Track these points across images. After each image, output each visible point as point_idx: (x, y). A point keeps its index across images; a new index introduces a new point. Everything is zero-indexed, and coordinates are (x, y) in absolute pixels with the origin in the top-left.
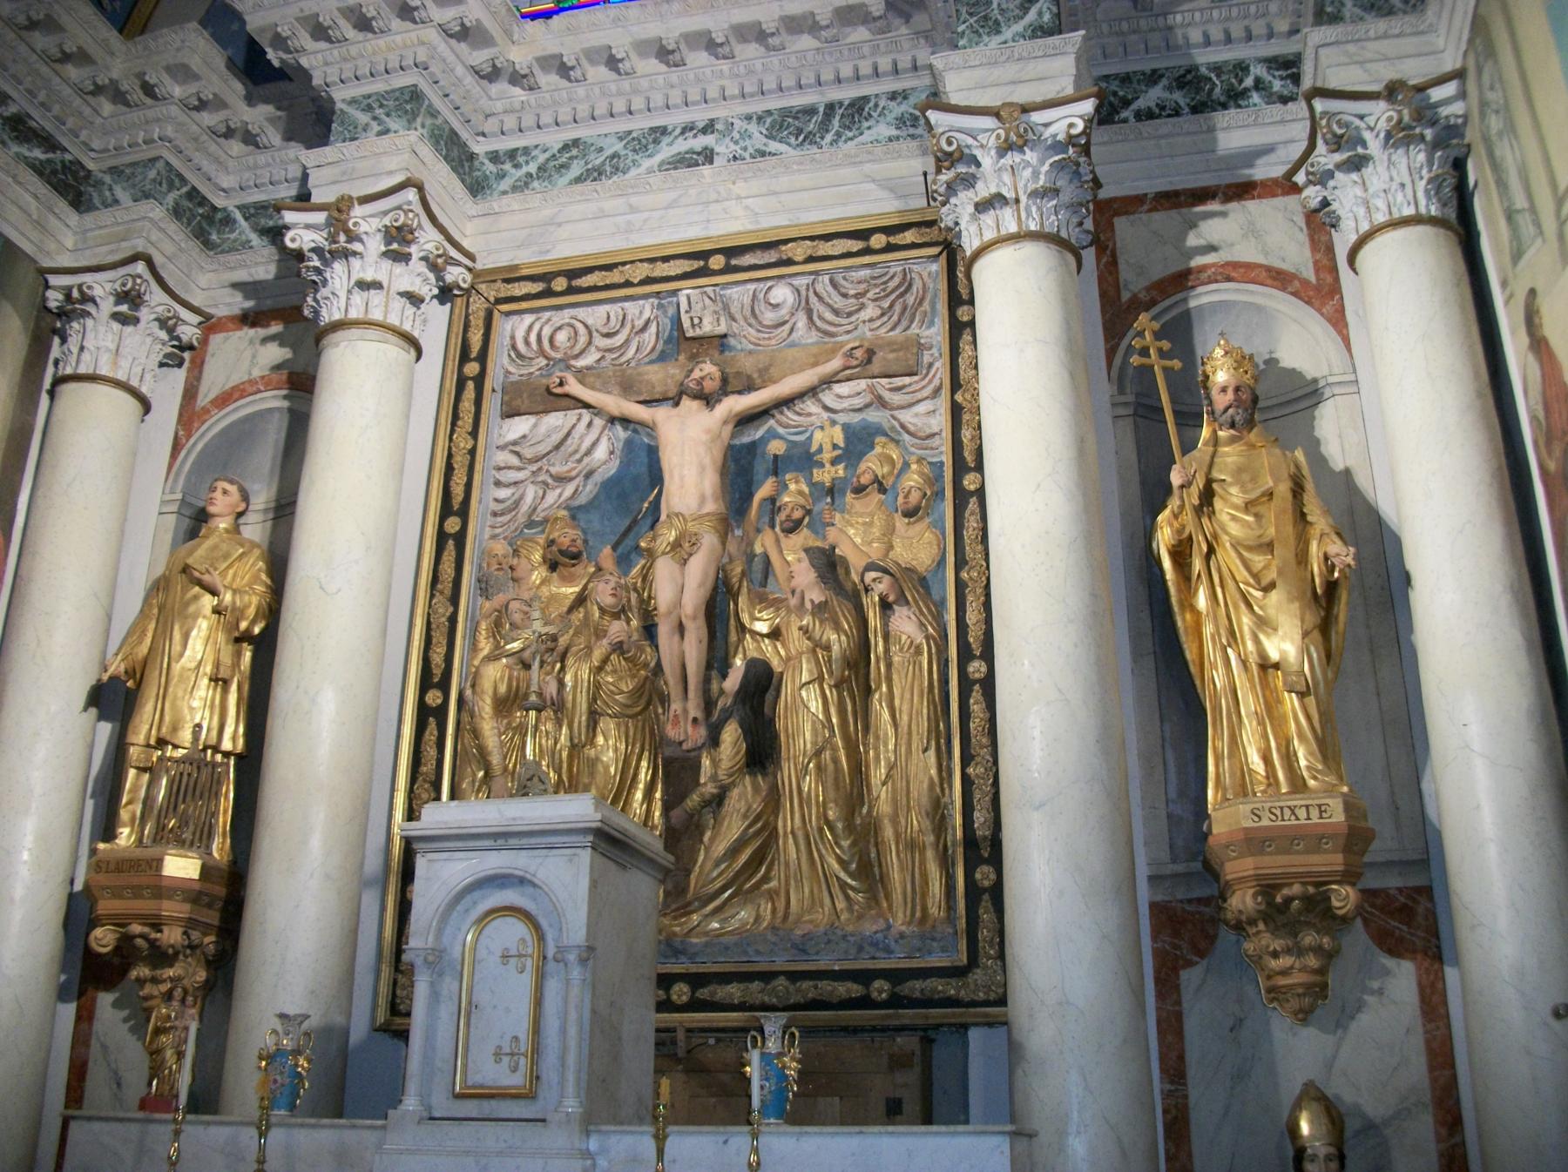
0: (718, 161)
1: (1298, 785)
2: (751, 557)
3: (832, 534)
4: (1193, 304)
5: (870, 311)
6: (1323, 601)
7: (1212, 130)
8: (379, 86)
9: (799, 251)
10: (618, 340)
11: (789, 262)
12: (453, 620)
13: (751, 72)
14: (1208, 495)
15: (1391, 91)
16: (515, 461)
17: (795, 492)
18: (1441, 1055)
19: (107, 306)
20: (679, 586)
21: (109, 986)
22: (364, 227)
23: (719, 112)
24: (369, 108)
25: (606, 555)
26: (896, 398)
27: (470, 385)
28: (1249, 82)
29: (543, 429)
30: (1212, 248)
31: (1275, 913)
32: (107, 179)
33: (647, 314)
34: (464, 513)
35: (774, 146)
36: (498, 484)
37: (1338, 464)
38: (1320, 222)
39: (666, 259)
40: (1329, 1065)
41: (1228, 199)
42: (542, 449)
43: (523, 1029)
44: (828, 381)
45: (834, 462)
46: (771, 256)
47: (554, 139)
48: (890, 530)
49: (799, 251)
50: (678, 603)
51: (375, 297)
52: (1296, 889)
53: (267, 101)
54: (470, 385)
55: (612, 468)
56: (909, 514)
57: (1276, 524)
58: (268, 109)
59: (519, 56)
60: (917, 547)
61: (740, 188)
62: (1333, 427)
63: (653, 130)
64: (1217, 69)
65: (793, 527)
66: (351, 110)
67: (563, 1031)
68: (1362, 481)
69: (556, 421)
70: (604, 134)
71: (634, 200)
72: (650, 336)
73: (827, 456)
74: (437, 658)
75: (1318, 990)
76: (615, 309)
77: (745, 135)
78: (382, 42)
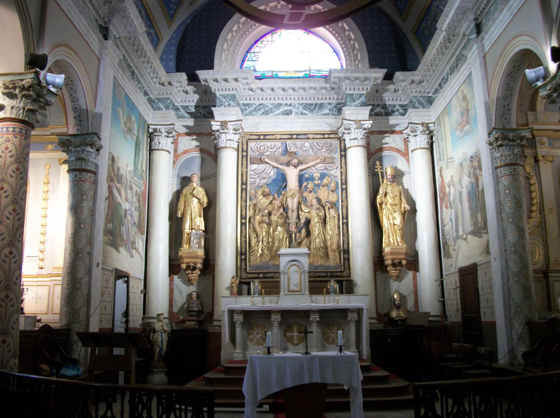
0: (293, 114)
1: (398, 245)
2: (303, 197)
3: (318, 194)
4: (383, 154)
5: (324, 150)
6: (403, 214)
7: (388, 119)
8: (227, 93)
9: (311, 136)
10: (274, 150)
11: (309, 138)
12: (246, 206)
13: (301, 95)
14: (386, 194)
15: (423, 124)
16: (254, 173)
17: (310, 185)
18: (415, 286)
19: (165, 134)
20: (292, 203)
21: (176, 274)
22: (230, 128)
23: (293, 102)
24: (225, 98)
26: (329, 168)
27: (245, 157)
28: (396, 109)
29: (259, 167)
30: (387, 144)
31: (394, 265)
32: (156, 101)
33: (280, 145)
34: (246, 184)
35: (305, 111)
36: (251, 178)
37: (406, 188)
38: (406, 141)
39: (284, 134)
40: (399, 287)
41: (390, 134)
42: (260, 172)
43: (298, 282)
44: (317, 164)
45: (318, 180)
46: (305, 137)
47: (257, 102)
48: (328, 194)
49: (311, 136)
50: (293, 206)
51: (232, 142)
52: (397, 261)
53: (192, 86)
54: (245, 157)
55: (274, 177)
56: (332, 191)
57: (397, 199)
58: (192, 87)
59: (253, 86)
60: (333, 198)
61: (298, 121)
62: (406, 180)
63: (279, 104)
64: (390, 105)
65: (310, 192)
66: (220, 97)
67: (305, 282)
68: (410, 191)
69: (262, 166)
70: (269, 103)
71: (276, 120)
72: (280, 150)
73: (317, 178)
74: (244, 214)
75: (398, 276)
76: (273, 143)
77: (298, 108)
78: (229, 84)
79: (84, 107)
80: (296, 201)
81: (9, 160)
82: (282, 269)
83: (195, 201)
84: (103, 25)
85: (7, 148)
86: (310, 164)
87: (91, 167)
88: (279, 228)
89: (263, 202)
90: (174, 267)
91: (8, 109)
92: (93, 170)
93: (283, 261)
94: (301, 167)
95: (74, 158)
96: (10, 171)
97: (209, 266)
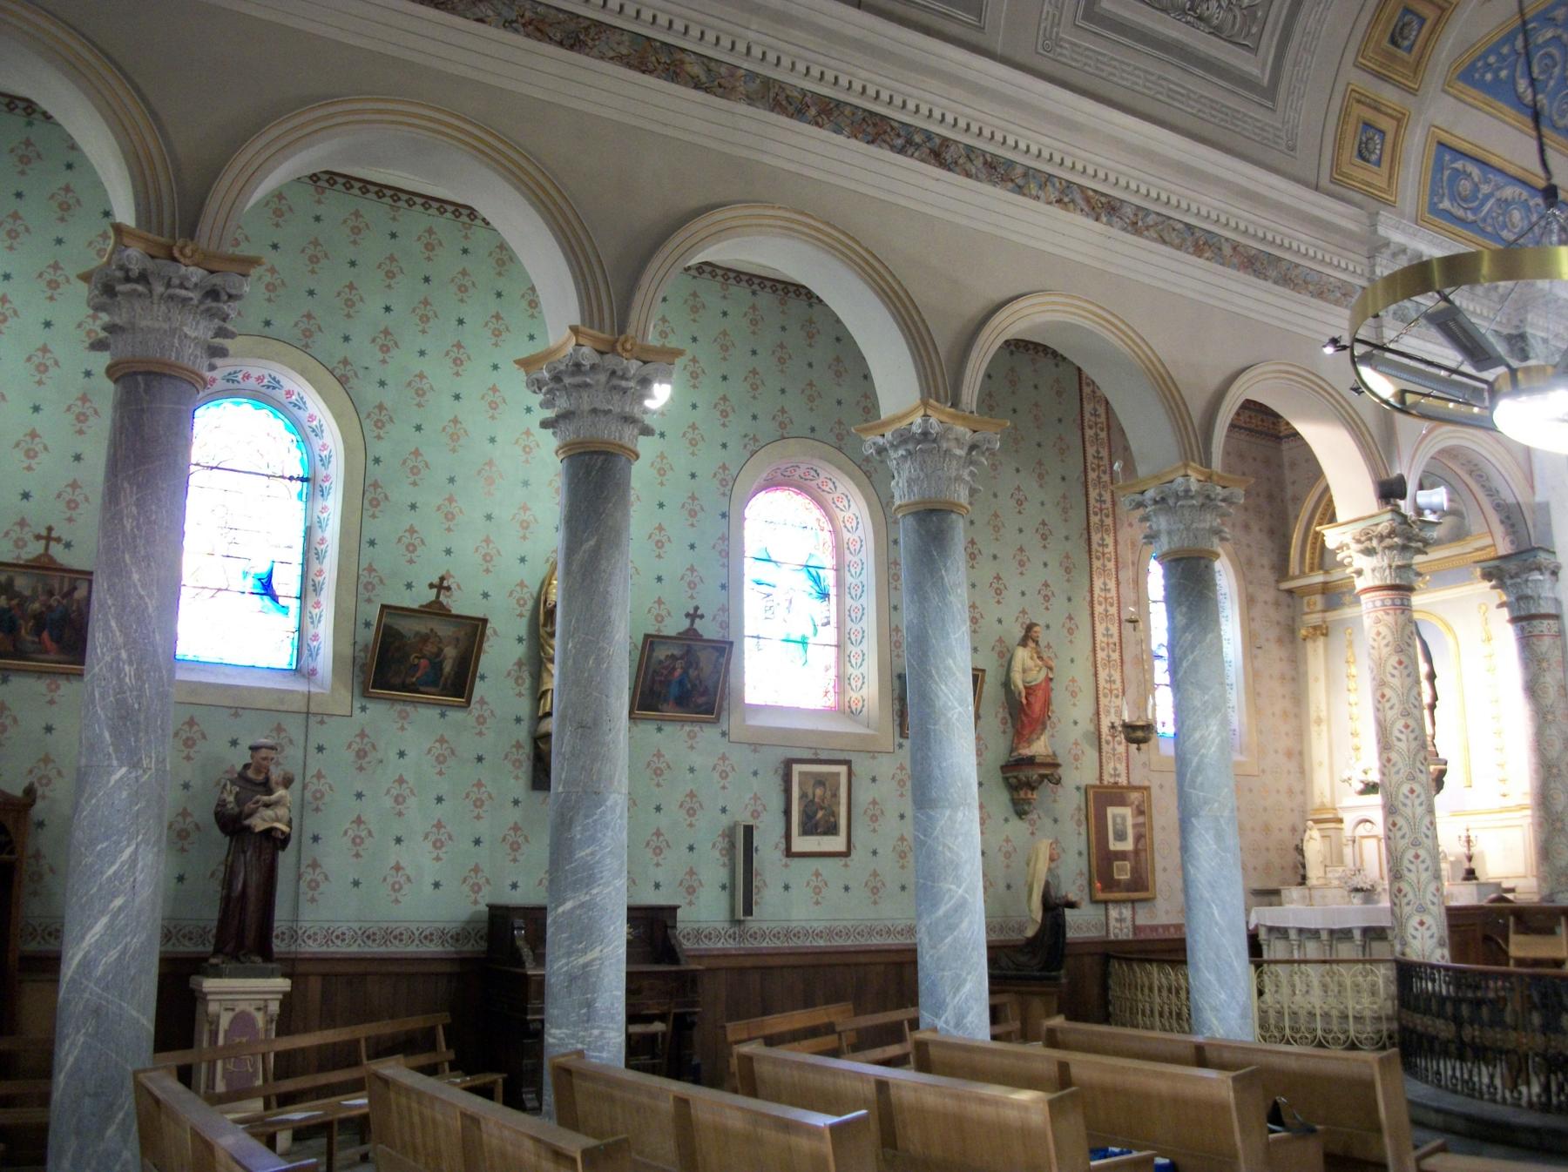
79: (1511, 500)
81: (1385, 651)
84: (1514, 332)
85: (1379, 634)
87: (1547, 608)
91: (1367, 572)
92: (1553, 611)
95: (1513, 599)
96: (1389, 669)
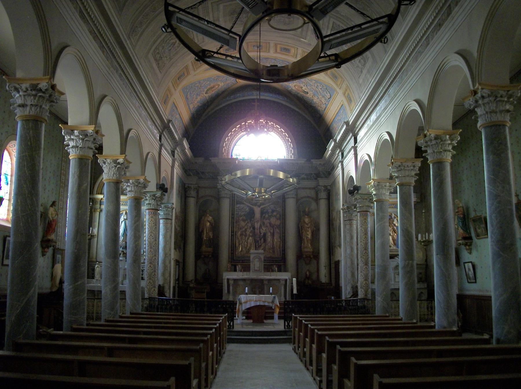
25: (249, 221)
65: (266, 219)
80: (259, 224)
82: (251, 260)
83: (208, 224)
86: (267, 205)
88: (250, 238)
89: (243, 224)
90: (198, 255)
93: (252, 256)
94: (262, 207)
97: (215, 256)
